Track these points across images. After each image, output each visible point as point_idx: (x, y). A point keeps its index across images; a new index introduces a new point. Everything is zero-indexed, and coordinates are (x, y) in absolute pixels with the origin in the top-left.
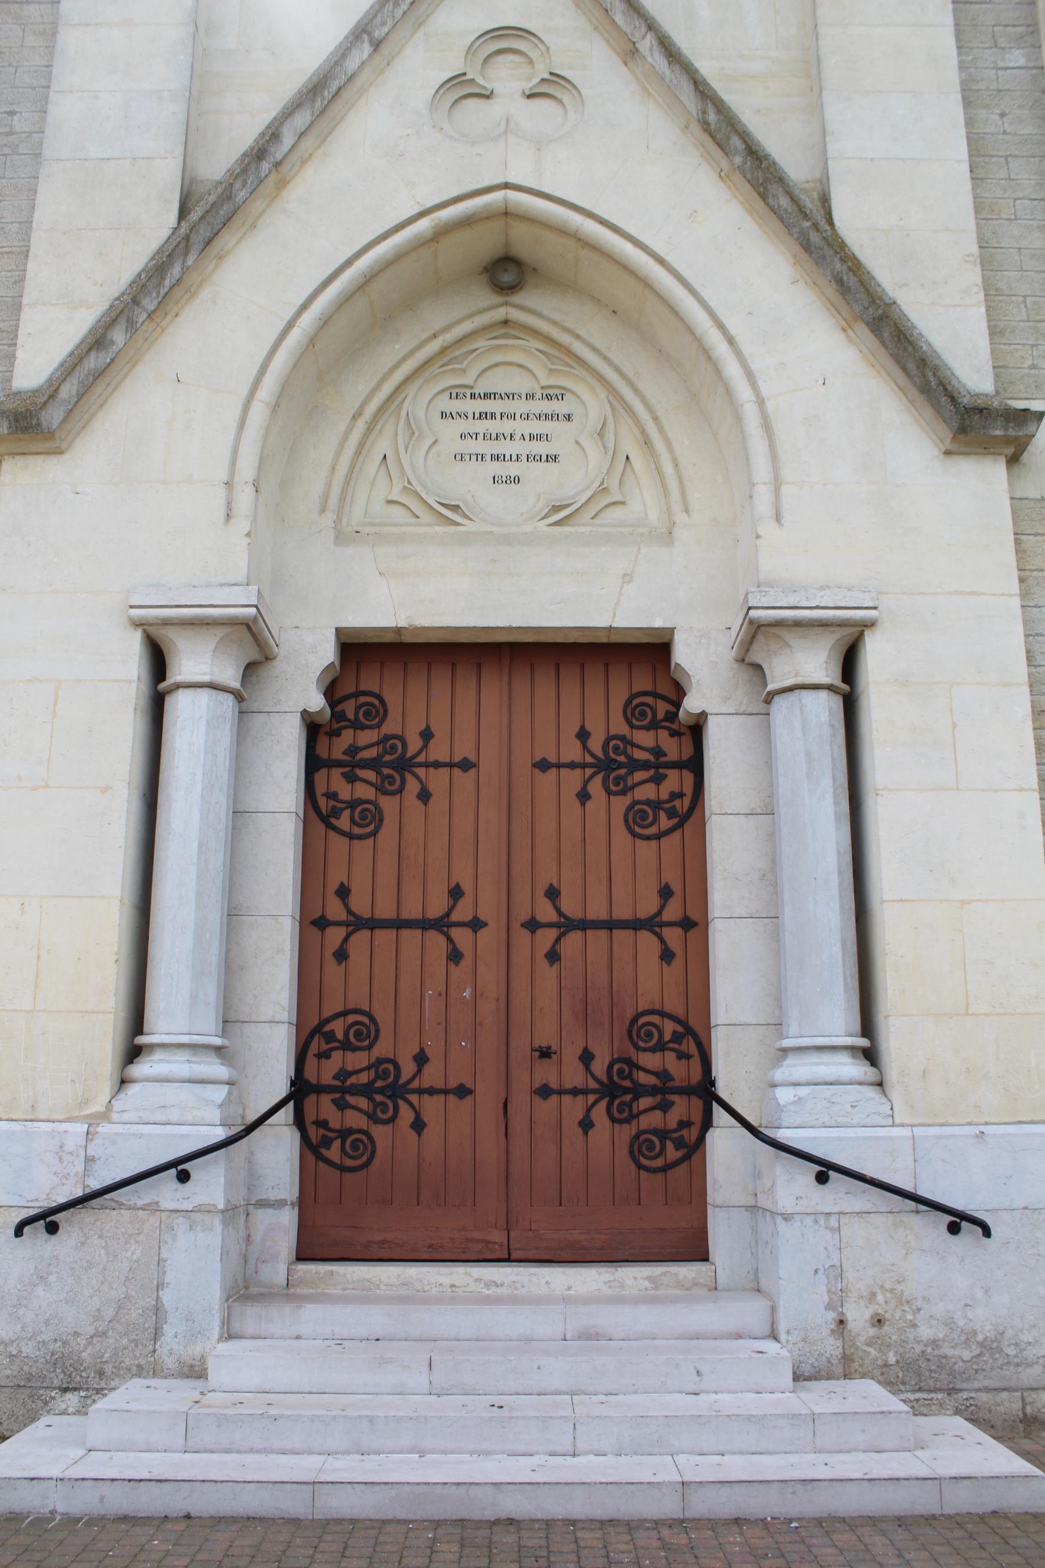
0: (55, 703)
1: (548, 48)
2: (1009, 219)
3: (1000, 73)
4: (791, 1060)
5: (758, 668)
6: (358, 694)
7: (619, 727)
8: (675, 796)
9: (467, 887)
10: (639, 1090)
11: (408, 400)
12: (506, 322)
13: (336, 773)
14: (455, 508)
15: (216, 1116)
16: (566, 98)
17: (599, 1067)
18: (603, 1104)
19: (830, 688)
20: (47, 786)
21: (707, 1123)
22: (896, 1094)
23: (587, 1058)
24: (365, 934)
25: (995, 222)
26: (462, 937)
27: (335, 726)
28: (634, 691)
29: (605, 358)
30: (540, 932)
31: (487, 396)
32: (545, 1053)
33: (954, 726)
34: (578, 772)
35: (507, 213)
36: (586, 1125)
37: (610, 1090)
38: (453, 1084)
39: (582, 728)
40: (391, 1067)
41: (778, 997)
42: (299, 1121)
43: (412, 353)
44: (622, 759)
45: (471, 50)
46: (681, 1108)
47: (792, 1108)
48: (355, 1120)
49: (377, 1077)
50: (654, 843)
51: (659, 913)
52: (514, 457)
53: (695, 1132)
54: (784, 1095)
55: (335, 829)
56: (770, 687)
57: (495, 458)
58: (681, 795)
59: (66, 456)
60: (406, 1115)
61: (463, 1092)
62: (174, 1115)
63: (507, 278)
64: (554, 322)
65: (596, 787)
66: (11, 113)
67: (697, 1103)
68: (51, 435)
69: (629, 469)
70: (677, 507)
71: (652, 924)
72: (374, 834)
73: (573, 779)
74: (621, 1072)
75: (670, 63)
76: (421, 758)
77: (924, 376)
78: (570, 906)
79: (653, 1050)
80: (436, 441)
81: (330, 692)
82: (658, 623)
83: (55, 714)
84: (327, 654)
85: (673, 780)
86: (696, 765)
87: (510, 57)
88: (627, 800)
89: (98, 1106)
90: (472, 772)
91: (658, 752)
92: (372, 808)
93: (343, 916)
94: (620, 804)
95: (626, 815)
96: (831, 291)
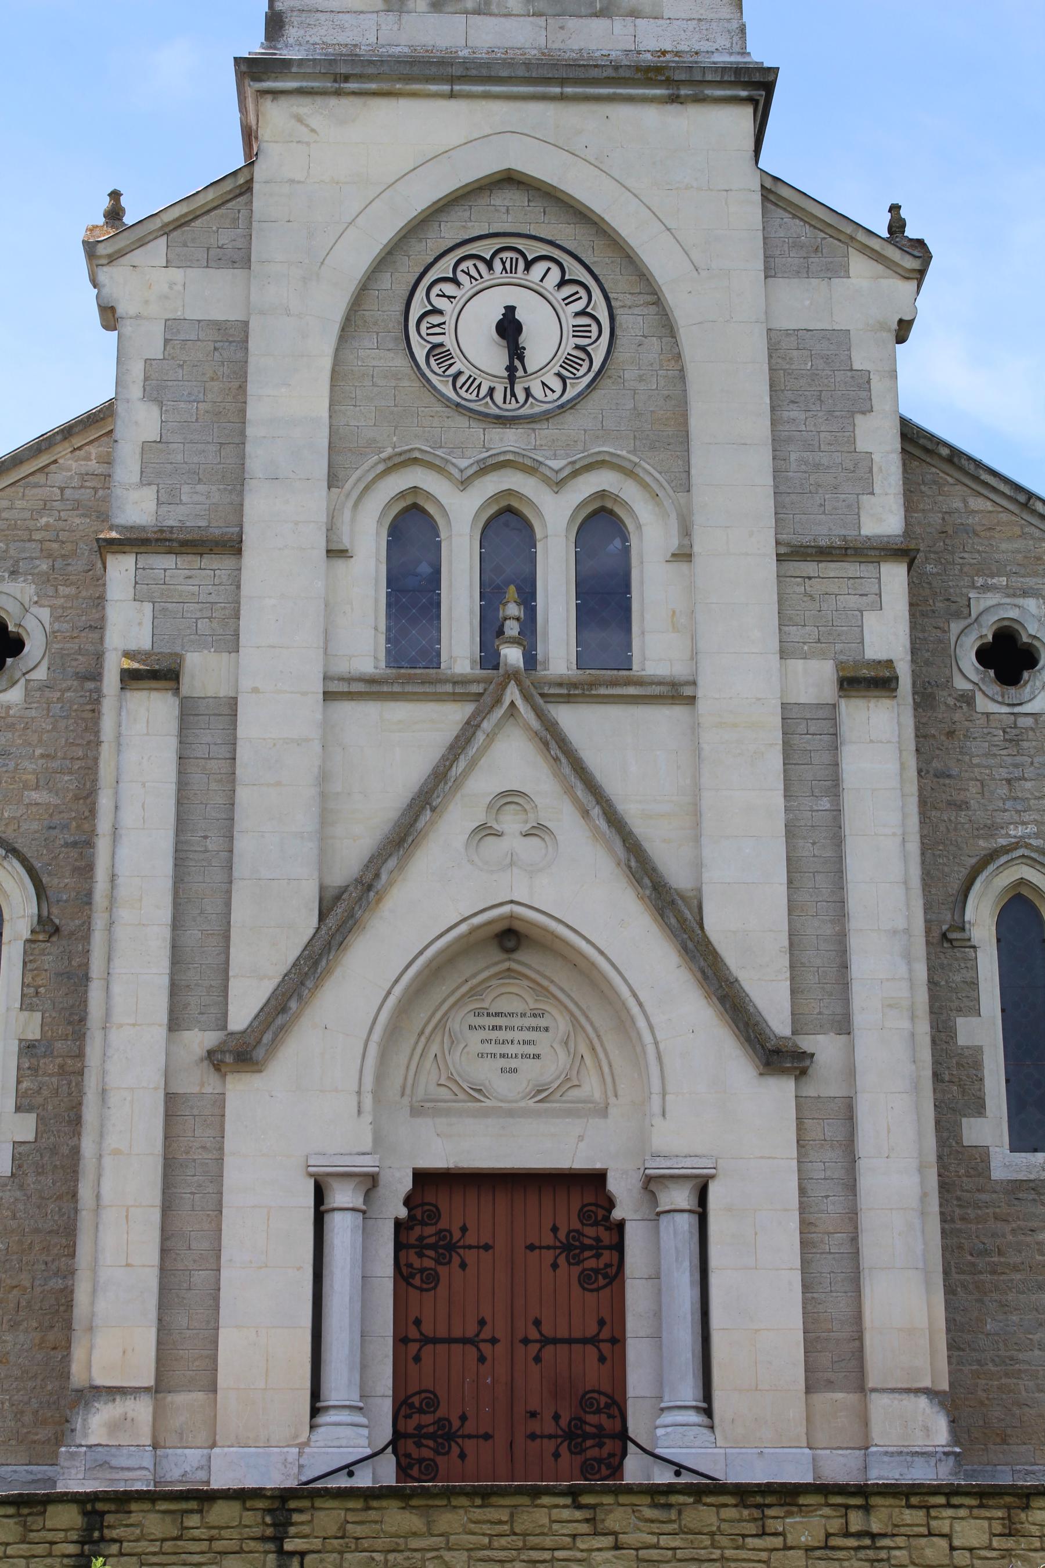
0: (268, 1220)
1: (536, 806)
2: (813, 916)
3: (814, 814)
4: (665, 1414)
5: (653, 1193)
6: (423, 1204)
7: (576, 1224)
8: (608, 1266)
9: (488, 1319)
10: (586, 1436)
11: (450, 1020)
12: (509, 970)
13: (412, 1251)
14: (479, 1091)
15: (366, 1442)
16: (547, 838)
17: (564, 1422)
18: (566, 1444)
19: (690, 1211)
20: (266, 1266)
21: (624, 1454)
22: (717, 1430)
23: (556, 1417)
24: (430, 1347)
25: (804, 918)
26: (486, 1348)
27: (411, 1224)
28: (585, 1203)
29: (569, 996)
30: (530, 1346)
31: (497, 1014)
32: (533, 1415)
33: (756, 1234)
34: (552, 1251)
35: (512, 917)
36: (556, 1455)
37: (569, 1435)
38: (481, 1432)
39: (554, 1225)
40: (447, 1423)
41: (660, 1381)
42: (395, 1452)
43: (453, 992)
44: (577, 1243)
45: (490, 806)
46: (609, 1446)
47: (663, 1438)
48: (427, 1453)
49: (439, 1429)
50: (595, 1293)
51: (598, 1334)
52: (514, 1056)
53: (617, 1459)
54: (660, 1432)
55: (412, 1285)
56: (658, 1210)
57: (503, 1056)
58: (611, 1265)
59: (263, 1074)
60: (455, 1450)
61: (487, 1437)
62: (344, 1442)
63: (510, 944)
64: (538, 972)
65: (562, 1260)
66: (206, 837)
67: (618, 1443)
68: (257, 1063)
69: (583, 1064)
70: (610, 1093)
71: (594, 1341)
72: (435, 1288)
73: (549, 1256)
74: (576, 1425)
75: (609, 826)
76: (461, 1243)
77: (747, 1032)
78: (547, 1330)
79: (594, 1413)
80: (466, 1046)
81: (407, 1202)
82: (598, 1166)
83: (268, 1226)
84: (407, 1184)
85: (607, 1256)
86: (619, 1247)
87: (513, 806)
88: (579, 1268)
89: (303, 1438)
90: (490, 1251)
91: (598, 1239)
92: (433, 1272)
93: (418, 1336)
94: (576, 1270)
95: (579, 1277)
96: (699, 975)
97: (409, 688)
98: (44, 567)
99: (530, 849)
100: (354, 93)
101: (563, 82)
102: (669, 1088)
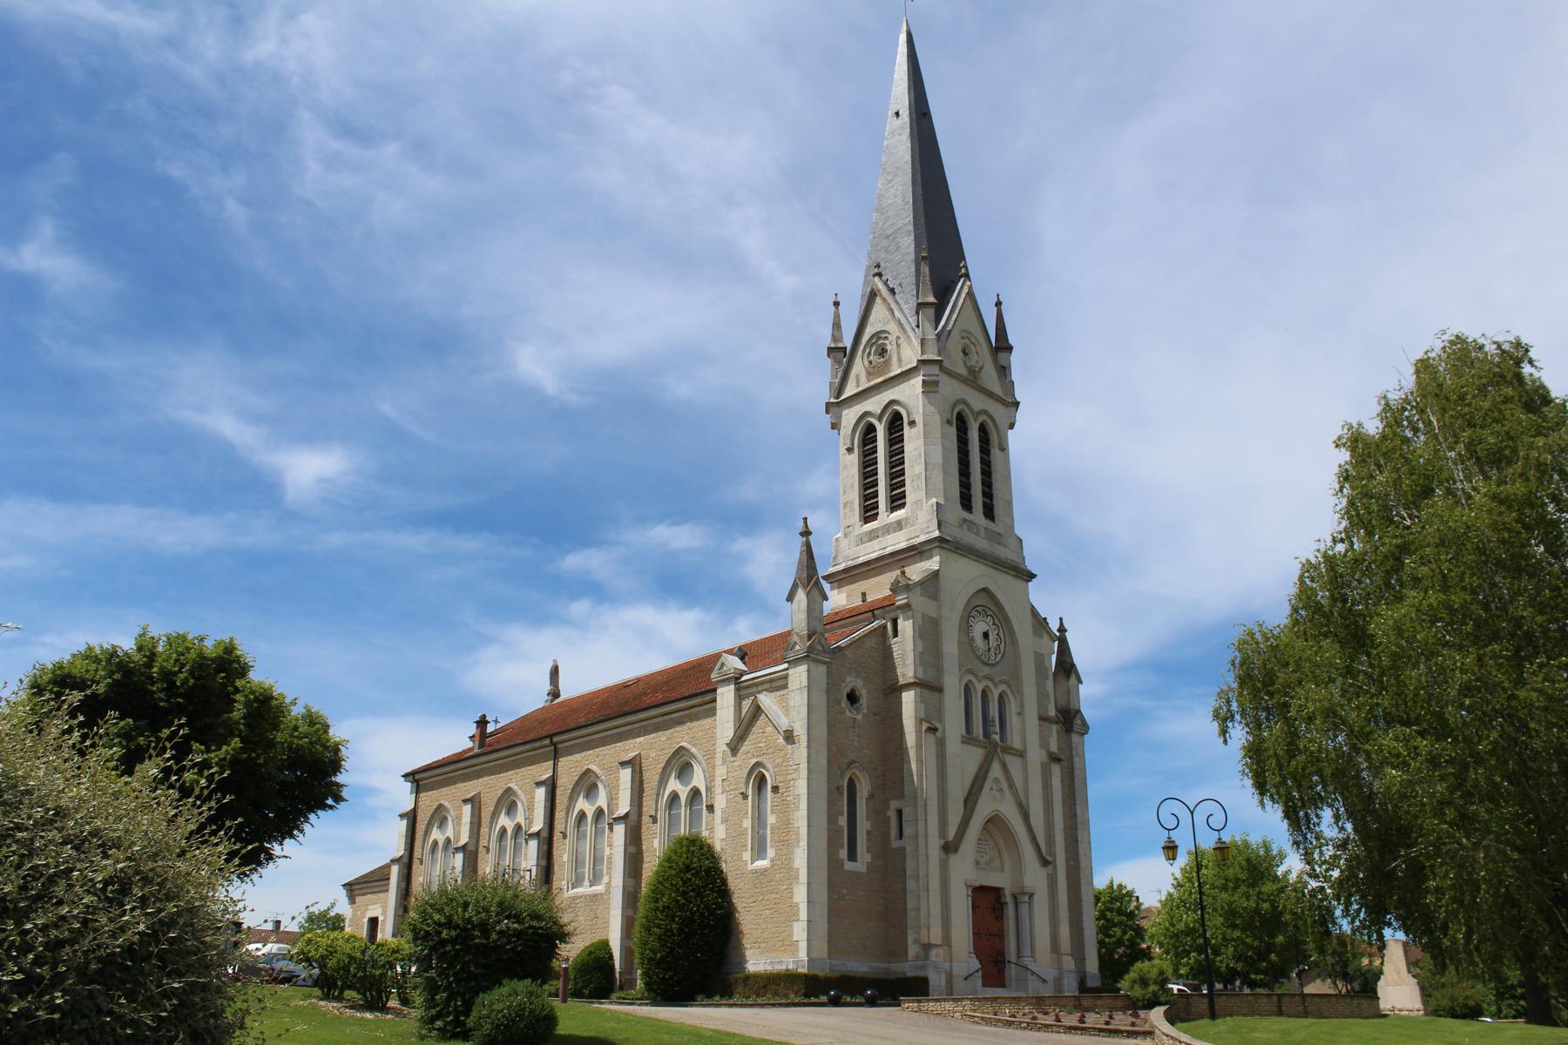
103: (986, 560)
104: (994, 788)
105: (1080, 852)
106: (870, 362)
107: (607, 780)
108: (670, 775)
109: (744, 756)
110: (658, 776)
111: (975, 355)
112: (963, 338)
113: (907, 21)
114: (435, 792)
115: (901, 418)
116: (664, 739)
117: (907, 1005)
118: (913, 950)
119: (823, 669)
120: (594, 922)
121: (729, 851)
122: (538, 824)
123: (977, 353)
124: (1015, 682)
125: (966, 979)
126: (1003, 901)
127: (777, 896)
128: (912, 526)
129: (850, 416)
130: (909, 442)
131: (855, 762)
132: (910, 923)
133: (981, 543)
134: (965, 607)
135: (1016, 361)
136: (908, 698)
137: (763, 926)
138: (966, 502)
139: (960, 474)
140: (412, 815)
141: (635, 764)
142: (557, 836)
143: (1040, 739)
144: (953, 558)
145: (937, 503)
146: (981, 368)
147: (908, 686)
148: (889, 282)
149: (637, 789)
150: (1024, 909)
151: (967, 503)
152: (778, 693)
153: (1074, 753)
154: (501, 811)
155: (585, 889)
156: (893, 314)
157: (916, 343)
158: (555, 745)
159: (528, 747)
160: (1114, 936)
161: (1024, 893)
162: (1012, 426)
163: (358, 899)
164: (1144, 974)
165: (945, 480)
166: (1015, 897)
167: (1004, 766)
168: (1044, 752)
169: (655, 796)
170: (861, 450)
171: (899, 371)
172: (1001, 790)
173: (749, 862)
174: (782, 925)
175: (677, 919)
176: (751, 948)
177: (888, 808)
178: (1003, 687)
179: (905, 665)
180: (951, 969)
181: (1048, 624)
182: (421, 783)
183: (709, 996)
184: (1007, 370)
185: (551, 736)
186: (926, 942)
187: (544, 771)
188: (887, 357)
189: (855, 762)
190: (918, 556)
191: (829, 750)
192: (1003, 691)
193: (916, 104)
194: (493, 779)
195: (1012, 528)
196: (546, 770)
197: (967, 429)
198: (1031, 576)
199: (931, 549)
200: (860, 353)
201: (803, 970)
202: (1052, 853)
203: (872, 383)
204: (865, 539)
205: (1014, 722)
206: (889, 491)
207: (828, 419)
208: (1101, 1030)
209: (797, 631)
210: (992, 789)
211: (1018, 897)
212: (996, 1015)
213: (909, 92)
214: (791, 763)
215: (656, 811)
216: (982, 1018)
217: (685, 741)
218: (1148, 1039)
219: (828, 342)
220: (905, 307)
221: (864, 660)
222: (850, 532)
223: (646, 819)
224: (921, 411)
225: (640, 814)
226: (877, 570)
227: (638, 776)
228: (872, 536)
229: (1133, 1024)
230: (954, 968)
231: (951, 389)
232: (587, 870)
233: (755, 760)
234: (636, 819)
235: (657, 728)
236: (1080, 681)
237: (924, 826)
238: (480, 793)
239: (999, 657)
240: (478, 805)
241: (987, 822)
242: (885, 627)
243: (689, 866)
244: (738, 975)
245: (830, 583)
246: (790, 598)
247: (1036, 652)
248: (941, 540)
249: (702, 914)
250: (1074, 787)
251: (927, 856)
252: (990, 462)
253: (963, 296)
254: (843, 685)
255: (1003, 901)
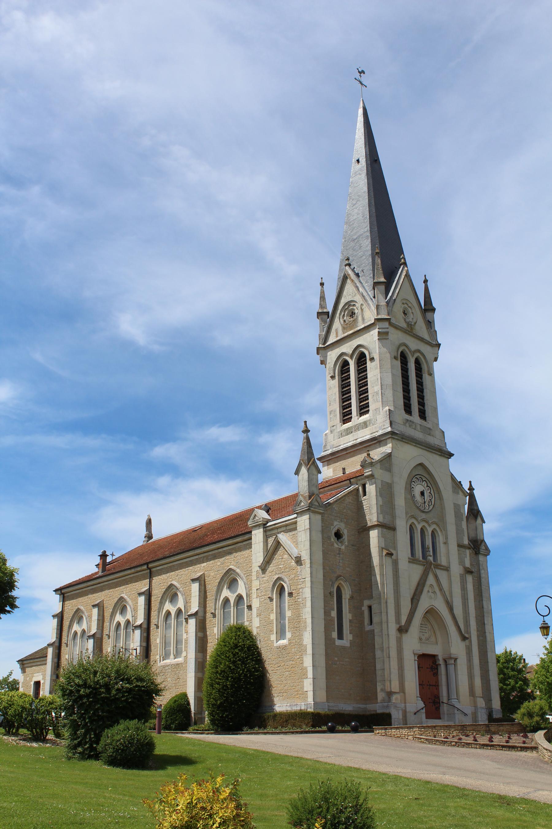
7: (432, 664)
97: (417, 562)
98: (345, 521)
99: (432, 595)
100: (403, 442)
101: (429, 448)
102: (452, 642)
103: (422, 445)
104: (430, 591)
105: (486, 631)
106: (345, 321)
107: (184, 591)
108: (223, 587)
109: (270, 574)
110: (216, 587)
111: (411, 314)
112: (403, 304)
113: (363, 100)
114: (75, 600)
115: (365, 356)
116: (219, 564)
117: (378, 731)
118: (381, 696)
119: (319, 517)
120: (177, 681)
121: (262, 634)
122: (140, 620)
123: (412, 313)
124: (441, 522)
125: (415, 714)
126: (437, 663)
127: (293, 663)
128: (373, 425)
129: (332, 355)
130: (371, 372)
131: (340, 576)
132: (378, 678)
133: (418, 435)
134: (409, 475)
135: (438, 318)
136: (374, 535)
137: (285, 682)
138: (408, 409)
139: (403, 391)
140: (60, 615)
141: (201, 580)
142: (153, 627)
143: (459, 559)
144: (400, 444)
145: (389, 410)
146: (415, 323)
147: (373, 527)
148: (355, 269)
149: (202, 595)
150: (451, 668)
151: (408, 409)
152: (291, 533)
153: (481, 568)
154: (117, 612)
155: (171, 661)
156: (358, 290)
157: (373, 308)
158: (150, 569)
159: (133, 571)
160: (509, 684)
161: (451, 658)
162: (436, 359)
163: (27, 670)
164: (530, 709)
165: (394, 395)
166: (445, 661)
167: (436, 577)
168: (461, 567)
169: (214, 600)
170: (340, 377)
171: (363, 326)
172: (434, 592)
173: (275, 641)
174: (297, 681)
175: (230, 679)
176: (277, 696)
177: (363, 605)
178: (434, 526)
179: (371, 514)
180: (405, 707)
181: (462, 485)
182: (65, 595)
183: (252, 728)
184: (432, 324)
185: (147, 564)
186: (389, 690)
187: (143, 586)
188: (355, 317)
189: (340, 576)
190: (378, 444)
191: (324, 569)
192: (434, 529)
193: (370, 154)
194: (111, 592)
195: (438, 424)
196: (145, 585)
197: (407, 362)
198: (451, 455)
199: (386, 439)
200: (338, 315)
201: (311, 710)
202: (468, 632)
203: (346, 334)
204: (344, 434)
205: (442, 549)
206: (358, 403)
207: (318, 358)
208: (503, 746)
209: (302, 493)
210: (428, 592)
211: (447, 661)
212: (435, 737)
213: (365, 147)
214: (300, 578)
215: (215, 610)
216: (427, 739)
217: (232, 565)
218: (534, 752)
219: (317, 309)
220: (365, 285)
221: (345, 511)
222: (334, 430)
223: (209, 615)
224: (377, 352)
225: (205, 612)
226: (352, 453)
227: (203, 588)
228: (348, 432)
229: (524, 742)
230: (407, 707)
231: (396, 336)
232: (172, 649)
233: (277, 576)
234: (203, 615)
235: (215, 557)
236: (483, 522)
237: (386, 617)
238: (103, 600)
239: (431, 507)
240: (102, 608)
241: (426, 613)
242: (358, 490)
243: (236, 645)
244: (270, 714)
245: (322, 462)
246: (297, 472)
247: (454, 503)
248: (392, 433)
249: (245, 675)
250: (481, 590)
251: (388, 635)
252: (422, 383)
253: (403, 277)
254: (332, 527)
255: (437, 663)
